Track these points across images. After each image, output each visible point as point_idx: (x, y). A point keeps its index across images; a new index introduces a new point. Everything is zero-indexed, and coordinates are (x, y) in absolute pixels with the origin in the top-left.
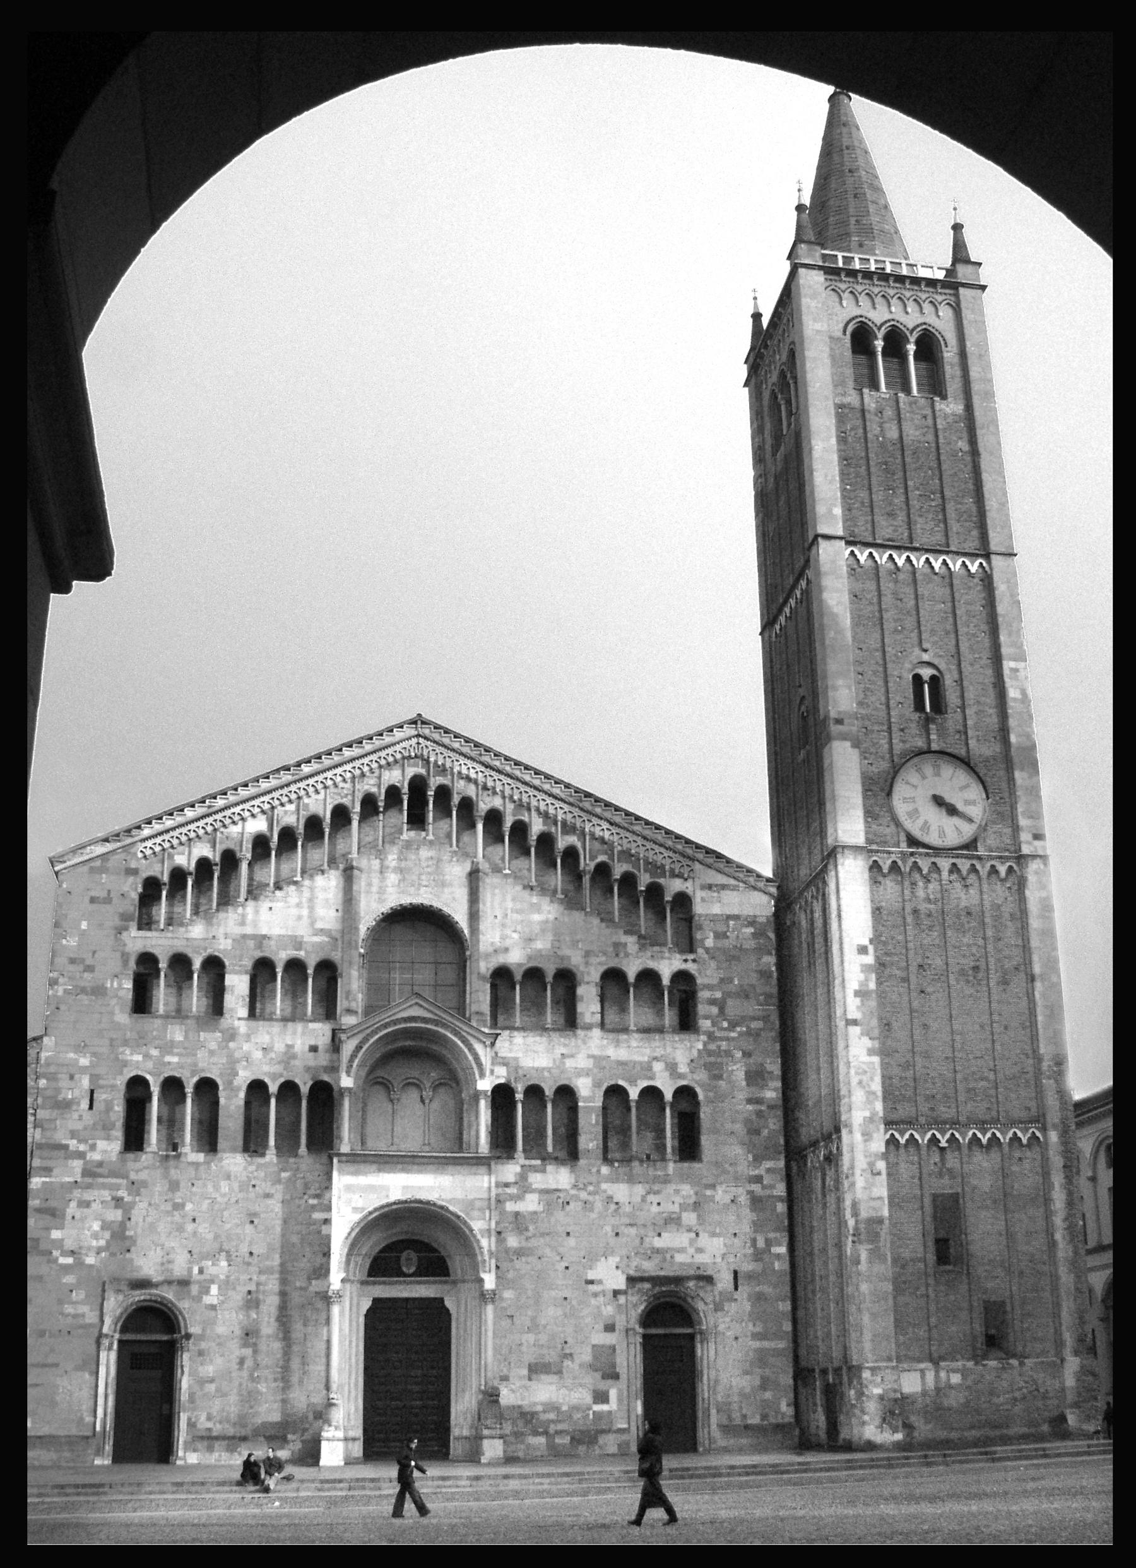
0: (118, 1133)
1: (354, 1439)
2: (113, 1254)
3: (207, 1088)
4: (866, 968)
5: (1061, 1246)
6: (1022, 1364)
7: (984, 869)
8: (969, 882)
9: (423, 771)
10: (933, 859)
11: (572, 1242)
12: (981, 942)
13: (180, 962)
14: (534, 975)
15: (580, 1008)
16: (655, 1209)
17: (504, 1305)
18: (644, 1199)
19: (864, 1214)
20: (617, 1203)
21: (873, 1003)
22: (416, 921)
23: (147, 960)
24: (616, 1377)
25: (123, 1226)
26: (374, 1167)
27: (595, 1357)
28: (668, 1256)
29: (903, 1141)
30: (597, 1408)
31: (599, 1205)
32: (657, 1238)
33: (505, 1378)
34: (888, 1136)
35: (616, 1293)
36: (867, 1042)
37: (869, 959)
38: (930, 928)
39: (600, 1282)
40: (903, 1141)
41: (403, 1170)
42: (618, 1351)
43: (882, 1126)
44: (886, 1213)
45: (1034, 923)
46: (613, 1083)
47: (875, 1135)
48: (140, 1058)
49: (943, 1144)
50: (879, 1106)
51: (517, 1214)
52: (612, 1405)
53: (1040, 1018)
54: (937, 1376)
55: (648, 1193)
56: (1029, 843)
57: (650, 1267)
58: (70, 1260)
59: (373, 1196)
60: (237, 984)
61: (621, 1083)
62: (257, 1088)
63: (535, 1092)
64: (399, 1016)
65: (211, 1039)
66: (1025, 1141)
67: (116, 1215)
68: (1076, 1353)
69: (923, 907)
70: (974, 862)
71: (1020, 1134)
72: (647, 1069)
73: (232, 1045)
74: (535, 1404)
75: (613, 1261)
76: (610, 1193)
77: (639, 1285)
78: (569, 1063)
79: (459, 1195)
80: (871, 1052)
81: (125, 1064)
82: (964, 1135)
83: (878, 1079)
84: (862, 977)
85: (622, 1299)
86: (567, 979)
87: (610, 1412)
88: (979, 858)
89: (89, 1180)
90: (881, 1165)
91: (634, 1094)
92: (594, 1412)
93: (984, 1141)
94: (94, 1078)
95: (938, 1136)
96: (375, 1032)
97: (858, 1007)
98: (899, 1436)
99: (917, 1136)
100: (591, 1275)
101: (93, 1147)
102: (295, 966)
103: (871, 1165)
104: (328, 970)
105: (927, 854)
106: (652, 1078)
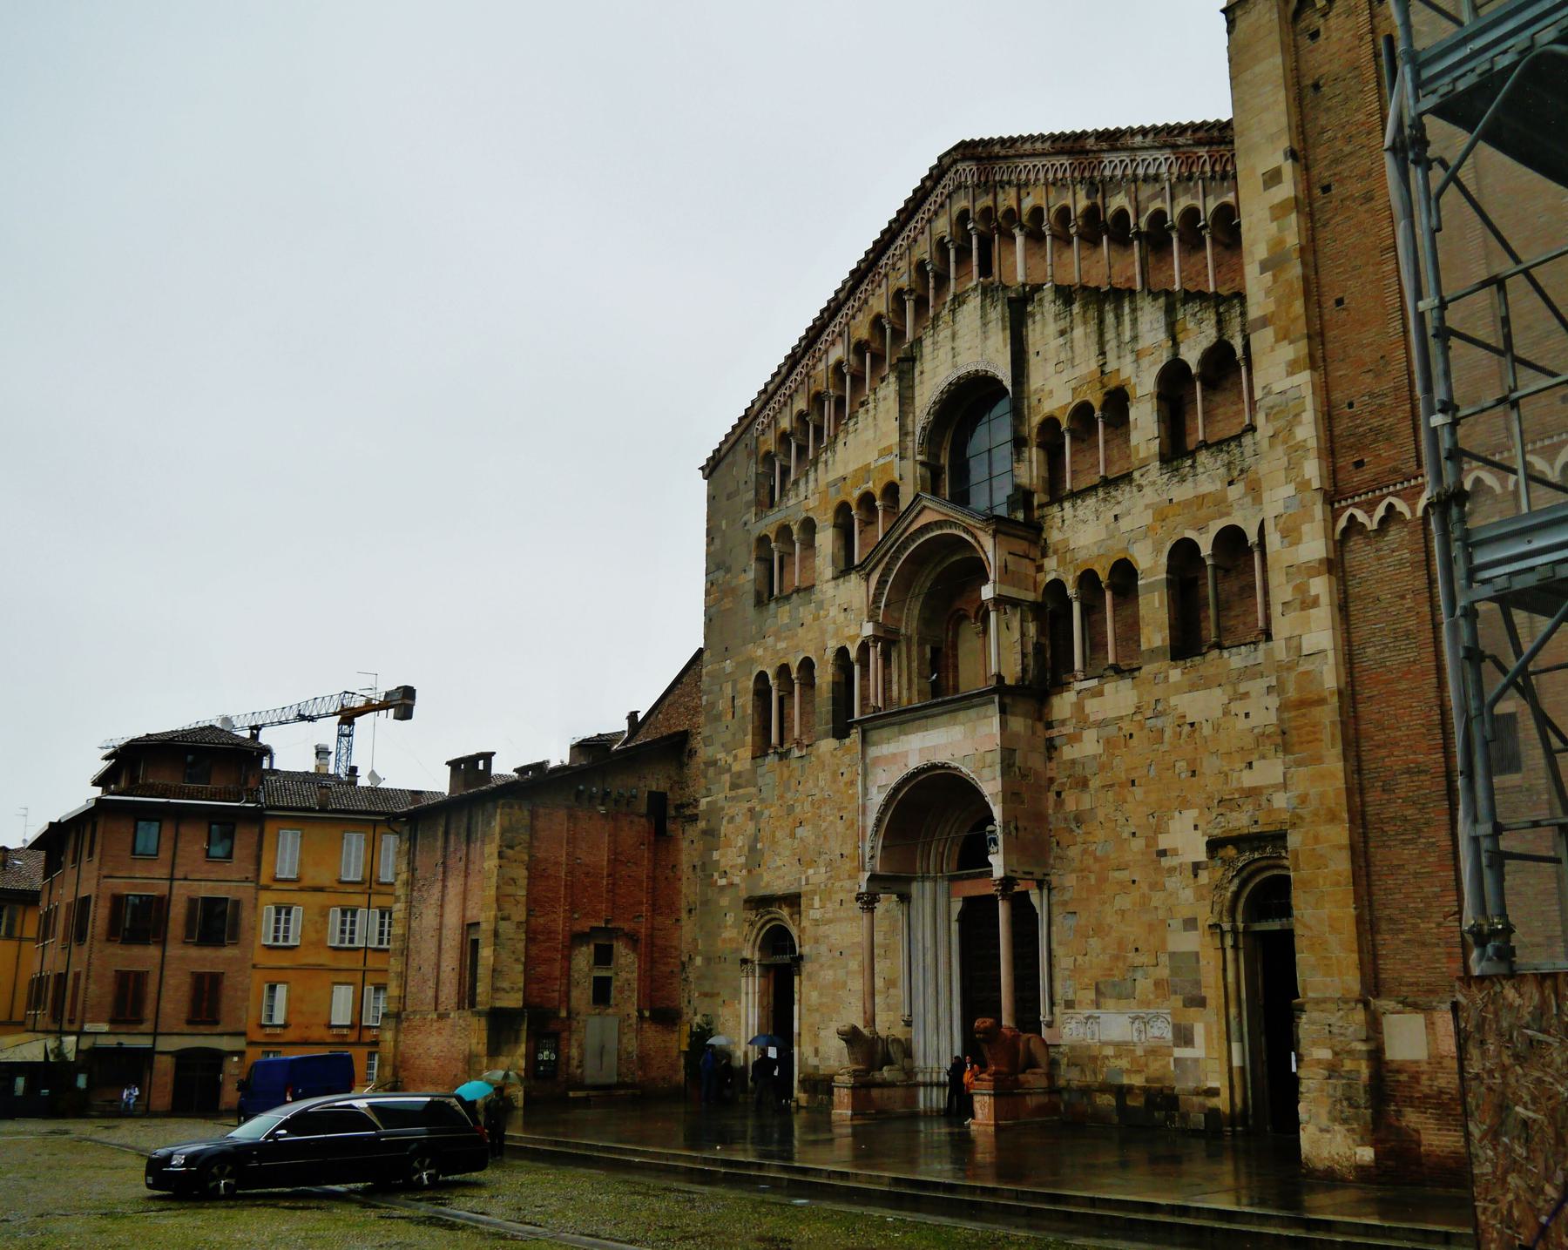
0: (749, 738)
1: (938, 1085)
2: (749, 871)
3: (807, 665)
4: (1279, 212)
9: (964, 203)
11: (1138, 791)
13: (784, 531)
14: (1082, 412)
15: (1135, 438)
16: (1242, 724)
17: (1067, 896)
18: (1226, 713)
19: (1292, 693)
20: (1192, 725)
21: (1295, 270)
22: (971, 399)
23: (763, 541)
24: (1201, 1002)
25: (756, 840)
26: (896, 729)
27: (1175, 971)
28: (1264, 803)
30: (1179, 1052)
31: (1168, 734)
32: (1246, 772)
33: (1069, 1004)
34: (1342, 523)
35: (1196, 867)
36: (1287, 352)
37: (1286, 190)
39: (1175, 852)
40: (1372, 525)
41: (918, 730)
42: (1203, 962)
43: (1318, 510)
46: (1176, 538)
47: (1305, 528)
48: (760, 652)
50: (1312, 470)
51: (1073, 762)
52: (1197, 1051)
55: (1230, 701)
57: (1240, 821)
58: (723, 882)
59: (894, 768)
60: (826, 539)
61: (1190, 534)
62: (842, 652)
63: (1088, 579)
64: (911, 530)
65: (806, 613)
67: (751, 828)
72: (1219, 503)
73: (822, 613)
74: (1105, 1044)
75: (1191, 815)
76: (1180, 710)
77: (1222, 853)
78: (1125, 524)
79: (968, 749)
80: (1293, 368)
81: (751, 661)
83: (1308, 416)
85: (1204, 877)
86: (1118, 400)
87: (1196, 1060)
89: (733, 793)
90: (1320, 586)
91: (1206, 549)
92: (1176, 1060)
94: (735, 683)
96: (895, 558)
97: (1268, 292)
98: (1366, 1154)
100: (1164, 842)
101: (735, 757)
102: (867, 500)
103: (1301, 589)
104: (892, 490)
106: (1228, 514)
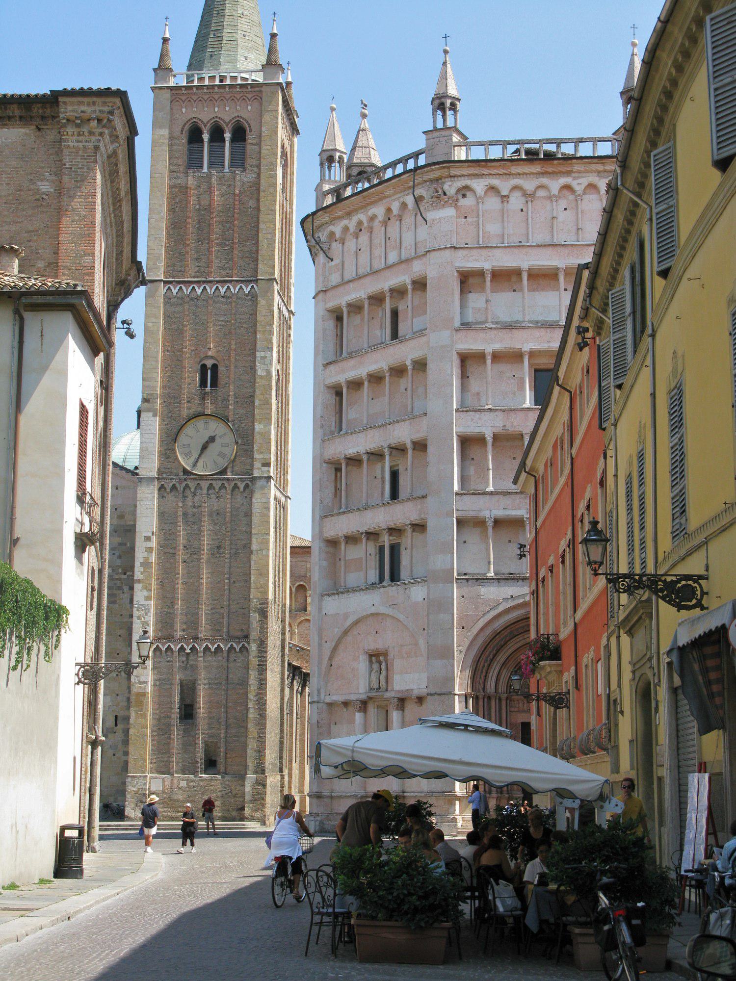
5: (252, 711)
6: (223, 777)
7: (229, 487)
8: (221, 494)
10: (198, 482)
12: (223, 530)
29: (163, 649)
38: (193, 523)
40: (163, 649)
44: (149, 689)
45: (256, 519)
49: (188, 651)
53: (252, 577)
54: (172, 782)
56: (259, 469)
66: (238, 650)
68: (255, 772)
69: (191, 511)
70: (224, 482)
71: (235, 645)
82: (200, 646)
84: (146, 555)
88: (228, 479)
93: (213, 650)
95: (185, 646)
99: (172, 646)
105: (195, 479)
